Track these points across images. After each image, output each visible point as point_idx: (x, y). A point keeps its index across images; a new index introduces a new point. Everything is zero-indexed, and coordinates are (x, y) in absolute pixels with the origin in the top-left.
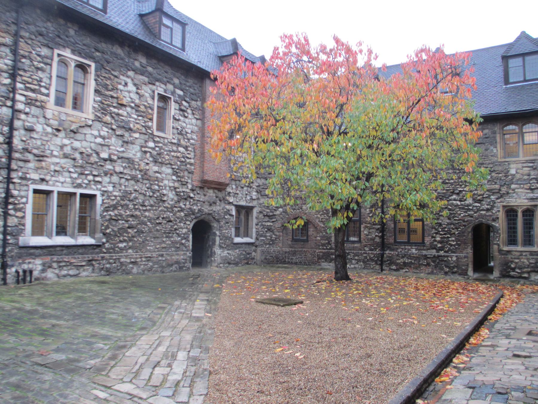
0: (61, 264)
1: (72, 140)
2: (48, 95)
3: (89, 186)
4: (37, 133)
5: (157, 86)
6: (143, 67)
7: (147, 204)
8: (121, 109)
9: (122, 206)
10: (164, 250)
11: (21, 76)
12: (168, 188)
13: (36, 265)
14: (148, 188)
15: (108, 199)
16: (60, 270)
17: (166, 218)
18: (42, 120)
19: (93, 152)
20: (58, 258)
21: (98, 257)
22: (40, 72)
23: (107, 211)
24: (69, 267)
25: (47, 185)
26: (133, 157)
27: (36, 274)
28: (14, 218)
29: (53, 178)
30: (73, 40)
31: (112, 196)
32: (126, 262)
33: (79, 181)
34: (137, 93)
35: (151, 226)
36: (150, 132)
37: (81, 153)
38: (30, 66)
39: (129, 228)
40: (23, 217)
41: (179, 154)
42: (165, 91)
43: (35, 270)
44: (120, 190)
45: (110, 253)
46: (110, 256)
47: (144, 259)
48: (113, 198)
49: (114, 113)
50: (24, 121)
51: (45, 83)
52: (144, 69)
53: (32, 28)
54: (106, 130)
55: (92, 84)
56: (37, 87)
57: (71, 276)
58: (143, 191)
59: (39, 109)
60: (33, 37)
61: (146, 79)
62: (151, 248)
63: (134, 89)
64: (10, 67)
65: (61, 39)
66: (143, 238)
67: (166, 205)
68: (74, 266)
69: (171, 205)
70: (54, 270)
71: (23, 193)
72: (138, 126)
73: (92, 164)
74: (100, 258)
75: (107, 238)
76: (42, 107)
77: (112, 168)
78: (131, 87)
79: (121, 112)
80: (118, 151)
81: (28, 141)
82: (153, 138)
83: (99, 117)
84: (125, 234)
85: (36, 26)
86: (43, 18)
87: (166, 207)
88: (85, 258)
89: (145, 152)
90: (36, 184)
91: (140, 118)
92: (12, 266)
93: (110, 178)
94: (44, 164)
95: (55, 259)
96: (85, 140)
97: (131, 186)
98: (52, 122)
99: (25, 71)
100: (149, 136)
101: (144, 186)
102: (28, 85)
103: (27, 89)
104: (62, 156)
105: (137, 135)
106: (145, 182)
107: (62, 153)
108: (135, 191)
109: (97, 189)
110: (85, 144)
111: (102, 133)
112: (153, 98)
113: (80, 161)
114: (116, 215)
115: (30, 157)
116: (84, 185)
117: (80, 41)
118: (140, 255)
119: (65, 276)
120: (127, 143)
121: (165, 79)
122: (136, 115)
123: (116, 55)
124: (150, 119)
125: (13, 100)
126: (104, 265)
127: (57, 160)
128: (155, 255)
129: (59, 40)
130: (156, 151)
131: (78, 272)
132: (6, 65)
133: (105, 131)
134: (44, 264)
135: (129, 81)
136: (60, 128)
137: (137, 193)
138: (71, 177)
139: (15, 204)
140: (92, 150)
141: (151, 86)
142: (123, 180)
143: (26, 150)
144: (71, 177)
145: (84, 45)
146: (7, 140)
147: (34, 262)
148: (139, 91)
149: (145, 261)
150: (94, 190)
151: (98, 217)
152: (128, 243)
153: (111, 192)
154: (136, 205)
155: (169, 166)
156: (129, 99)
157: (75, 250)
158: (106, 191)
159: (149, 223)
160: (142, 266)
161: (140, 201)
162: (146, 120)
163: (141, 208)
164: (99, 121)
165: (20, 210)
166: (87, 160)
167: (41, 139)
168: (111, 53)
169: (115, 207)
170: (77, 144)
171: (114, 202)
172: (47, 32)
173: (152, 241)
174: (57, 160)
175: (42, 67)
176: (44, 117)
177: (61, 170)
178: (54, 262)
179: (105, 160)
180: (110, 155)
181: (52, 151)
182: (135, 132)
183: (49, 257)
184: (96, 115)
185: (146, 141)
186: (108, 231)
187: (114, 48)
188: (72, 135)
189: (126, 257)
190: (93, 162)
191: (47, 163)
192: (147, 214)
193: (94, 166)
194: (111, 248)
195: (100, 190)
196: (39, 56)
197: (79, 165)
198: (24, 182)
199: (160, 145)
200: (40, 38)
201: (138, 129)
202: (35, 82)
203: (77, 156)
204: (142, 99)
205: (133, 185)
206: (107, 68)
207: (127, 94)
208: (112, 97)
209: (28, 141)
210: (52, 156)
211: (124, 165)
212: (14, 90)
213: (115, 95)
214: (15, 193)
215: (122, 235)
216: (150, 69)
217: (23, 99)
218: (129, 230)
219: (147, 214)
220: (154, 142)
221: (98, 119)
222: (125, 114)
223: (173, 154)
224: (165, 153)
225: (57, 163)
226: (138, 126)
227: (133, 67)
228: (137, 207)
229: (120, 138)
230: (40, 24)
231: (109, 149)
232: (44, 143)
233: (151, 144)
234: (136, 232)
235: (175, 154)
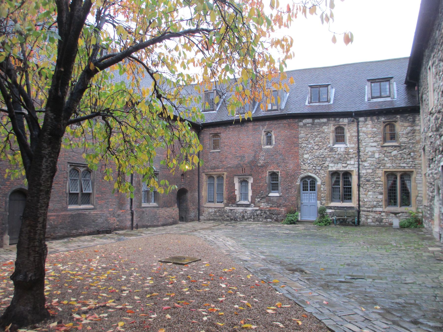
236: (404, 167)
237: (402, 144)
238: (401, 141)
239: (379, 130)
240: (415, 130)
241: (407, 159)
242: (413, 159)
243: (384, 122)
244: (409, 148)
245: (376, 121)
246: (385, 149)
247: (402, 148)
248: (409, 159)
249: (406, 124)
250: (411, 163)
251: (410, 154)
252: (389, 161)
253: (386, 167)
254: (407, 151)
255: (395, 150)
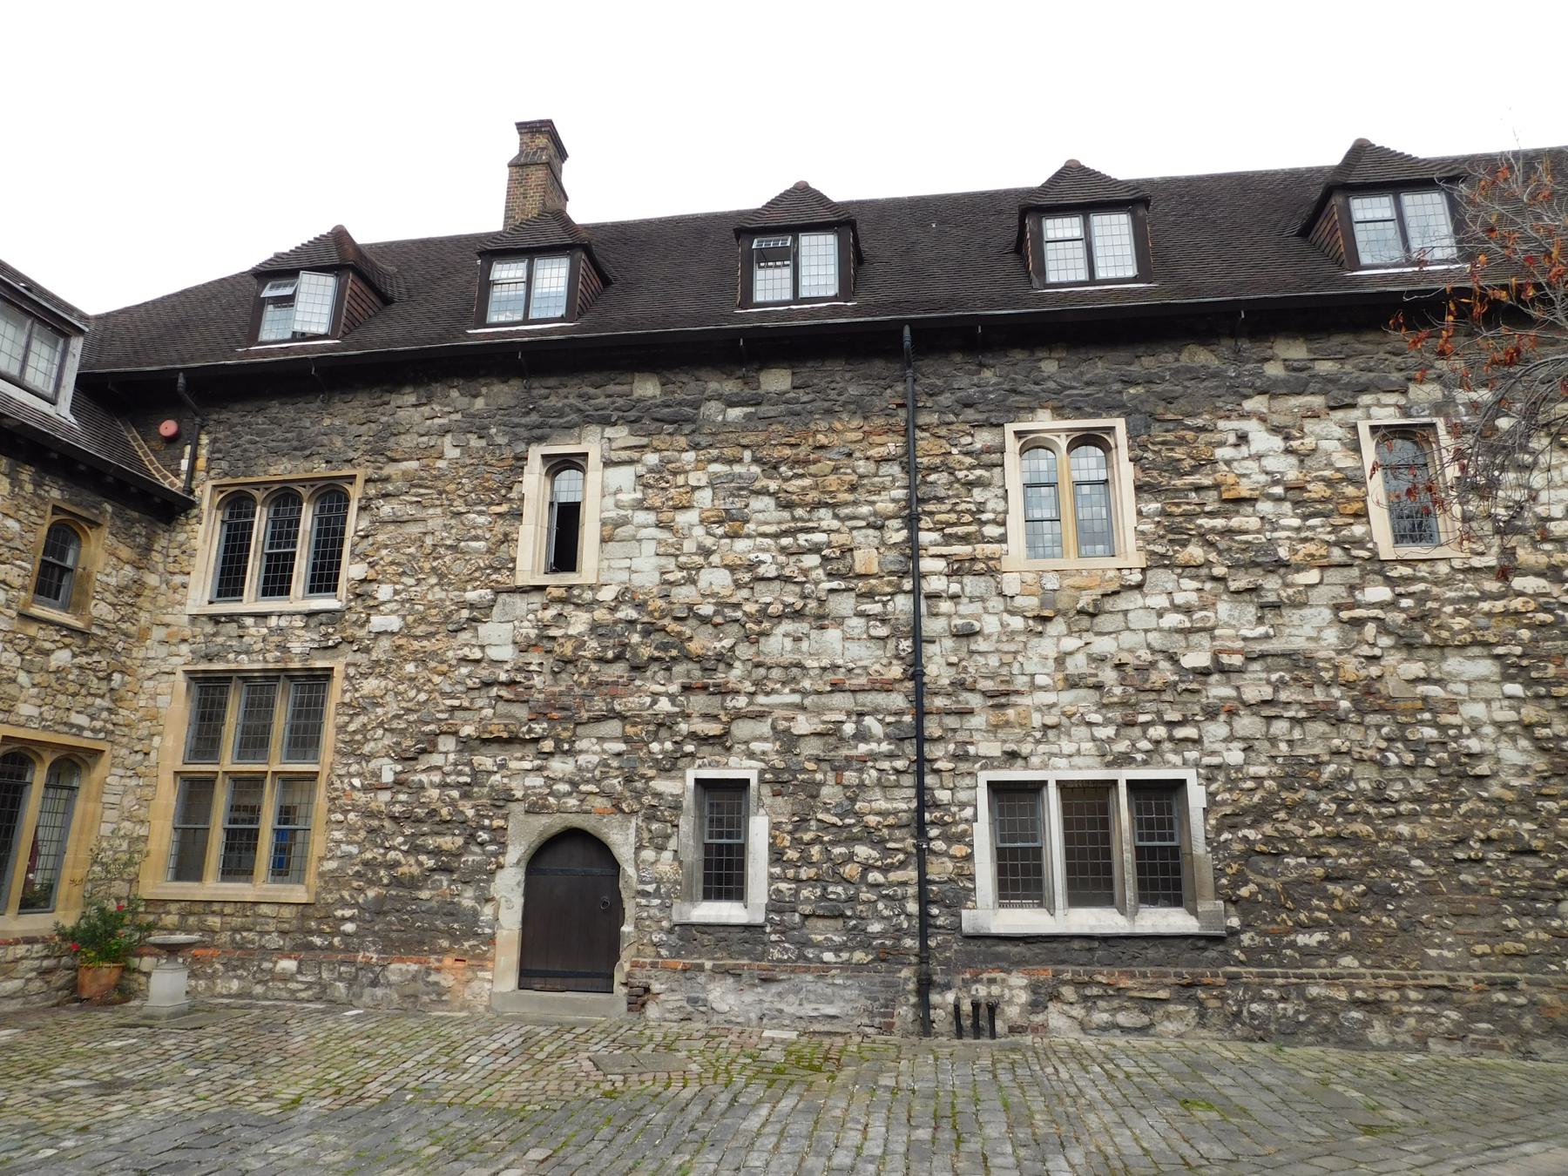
0: (1088, 992)
1: (1088, 637)
2: (1002, 539)
3: (1156, 758)
4: (987, 637)
5: (1368, 407)
6: (1295, 370)
7: (1396, 796)
8: (1237, 512)
9: (1291, 809)
10: (1517, 964)
11: (931, 514)
12: (1488, 730)
13: (1011, 988)
14: (1389, 740)
15: (1230, 790)
16: (1089, 1010)
17: (1502, 839)
18: (996, 603)
19: (1159, 657)
20: (1074, 973)
21: (1215, 975)
22: (976, 492)
23: (1233, 828)
24: (1116, 1003)
25: (1026, 767)
26: (1312, 645)
27: (1012, 1012)
28: (945, 859)
29: (1042, 748)
30: (1052, 385)
31: (1244, 779)
32: (1330, 999)
33: (1122, 746)
34: (1289, 451)
35: (1430, 871)
36: (1365, 554)
37: (1119, 666)
38: (951, 484)
39: (1328, 878)
40: (969, 858)
41: (1517, 604)
42: (1405, 411)
43: (1010, 1002)
44: (1273, 758)
45: (1262, 964)
46: (1259, 975)
47: (1413, 995)
48: (1250, 784)
49: (1213, 530)
50: (949, 616)
51: (994, 511)
52: (1304, 375)
53: (946, 399)
54: (1196, 584)
55: (1126, 473)
56: (972, 528)
57: (1125, 1030)
58: (1367, 753)
59: (983, 578)
60: (952, 418)
61: (1317, 401)
62: (1446, 953)
63: (1277, 442)
64: (903, 503)
65: (1021, 393)
66: (1402, 914)
67: (1495, 789)
68: (1131, 998)
69: (1521, 790)
70: (1065, 1007)
71: (962, 796)
72: (1311, 548)
73: (1159, 691)
74: (1221, 980)
75: (1243, 914)
76: (992, 572)
77: (1233, 693)
78: (1262, 439)
79: (1235, 522)
80: (1245, 639)
81: (964, 663)
82: (1380, 573)
83: (1163, 556)
84: (1315, 902)
85: (952, 390)
86: (967, 367)
87: (1498, 801)
88: (1166, 975)
89: (1358, 623)
90: (994, 768)
91: (1312, 522)
92: (947, 987)
93: (1229, 724)
94: (1011, 713)
95: (1068, 976)
96: (1128, 629)
97: (1316, 740)
98: (1019, 602)
99: (940, 500)
100: (1363, 569)
101: (1373, 734)
102: (948, 531)
103: (948, 539)
104: (1060, 684)
105: (1312, 576)
106: (1371, 719)
107: (1060, 676)
108: (1337, 753)
109: (1185, 763)
110: (1127, 639)
111: (1180, 599)
112: (1356, 448)
113: (1118, 691)
114: (1268, 839)
115: (975, 700)
116: (1139, 757)
117: (1074, 378)
118: (1389, 977)
119: (1105, 1028)
120: (1276, 606)
121: (1396, 376)
122: (1296, 515)
123: (1195, 374)
124: (1356, 515)
125: (919, 576)
126: (1240, 1003)
127: (1050, 698)
128: (1471, 983)
129: (1017, 398)
130: (1403, 610)
131: (1145, 1019)
132: (893, 500)
133: (1188, 591)
134: (1034, 988)
135: (1252, 427)
136: (1046, 613)
137: (1348, 761)
138: (1094, 739)
139: (946, 824)
140: (1153, 651)
141: (1339, 415)
142: (1280, 727)
143: (960, 685)
144: (1094, 739)
145: (1088, 384)
146: (912, 670)
147: (1004, 980)
148: (1295, 444)
149: (1419, 1002)
150: (1175, 766)
151: (1200, 848)
152: (1333, 932)
153: (1238, 769)
154: (1347, 800)
155: (1476, 650)
156: (1263, 478)
157: (1133, 949)
158: (1218, 767)
159: (1416, 862)
160: (1411, 1022)
161: (1364, 785)
162: (1338, 521)
163: (1371, 810)
164: (1166, 566)
165: (961, 838)
166: (1137, 683)
167: (997, 651)
168: (1176, 372)
169: (1260, 814)
170: (1103, 645)
171: (1256, 799)
172: (983, 393)
173: (1444, 928)
174: (1050, 698)
175: (980, 477)
176: (1001, 594)
177: (1064, 720)
178: (1065, 983)
179: (1205, 673)
180: (1216, 656)
181: (1033, 676)
182: (1299, 569)
183: (1050, 970)
184: (1153, 553)
185: (1352, 588)
186: (1244, 892)
187: (1192, 355)
188: (1085, 622)
189: (1332, 980)
190: (1158, 685)
191: (1020, 709)
192: (1403, 828)
193: (1167, 697)
194: (1266, 948)
195: (1197, 765)
196: (967, 454)
197: (1115, 699)
198: (964, 767)
199: (1419, 587)
200: (970, 414)
201: (1312, 556)
202: (968, 518)
203: (1108, 675)
204: (1308, 462)
205: (1324, 737)
206: (1169, 416)
207: (1252, 465)
208: (1198, 489)
209: (964, 663)
210: (1034, 688)
211: (1274, 677)
212: (913, 550)
213: (1207, 481)
214: (943, 796)
215: (1301, 904)
216: (1325, 367)
217: (941, 565)
218: (1331, 888)
219: (1403, 828)
220: (1390, 582)
221: (1159, 562)
222: (1254, 523)
223: (1485, 606)
224: (1449, 609)
225: (1053, 705)
226: (1311, 548)
227: (1258, 383)
228: (1352, 807)
229: (1247, 597)
230: (963, 381)
231: (1213, 638)
232: (1008, 658)
233: (1378, 592)
234: (1364, 894)
235: (1499, 606)
236: (81, 728)
237: (95, 630)
238: (95, 613)
239: (30, 536)
240: (143, 585)
241: (95, 695)
242: (114, 701)
243: (56, 510)
244: (112, 650)
245: (29, 488)
246: (32, 630)
247: (92, 644)
248: (102, 697)
249: (125, 552)
250: (105, 715)
251: (109, 678)
252: (34, 691)
253: (12, 718)
254: (104, 663)
255: (67, 646)
